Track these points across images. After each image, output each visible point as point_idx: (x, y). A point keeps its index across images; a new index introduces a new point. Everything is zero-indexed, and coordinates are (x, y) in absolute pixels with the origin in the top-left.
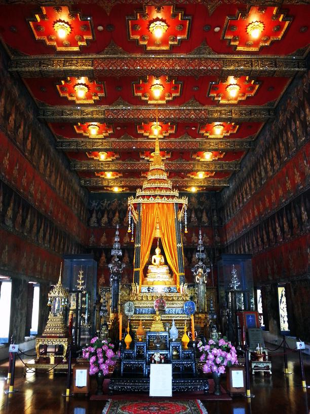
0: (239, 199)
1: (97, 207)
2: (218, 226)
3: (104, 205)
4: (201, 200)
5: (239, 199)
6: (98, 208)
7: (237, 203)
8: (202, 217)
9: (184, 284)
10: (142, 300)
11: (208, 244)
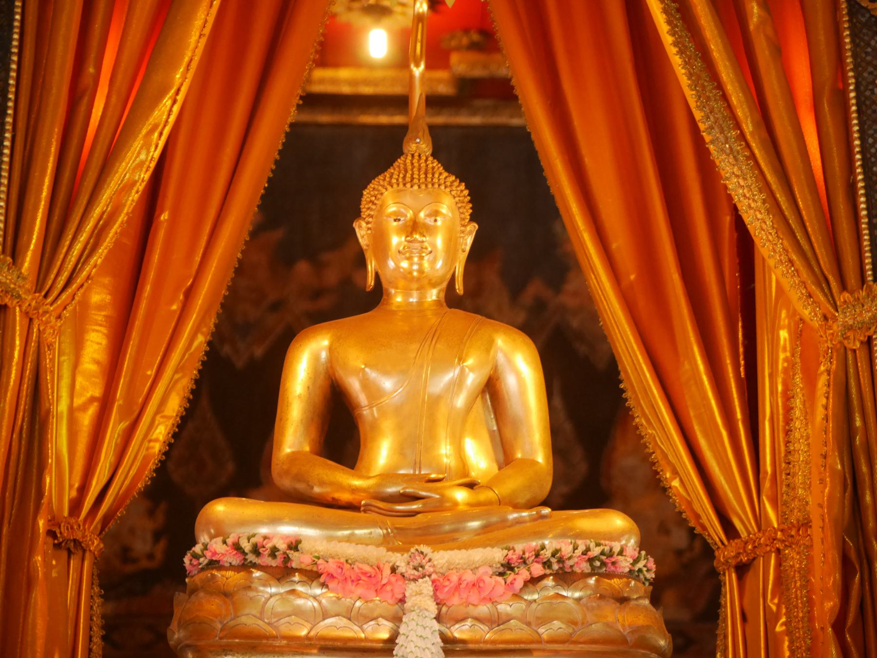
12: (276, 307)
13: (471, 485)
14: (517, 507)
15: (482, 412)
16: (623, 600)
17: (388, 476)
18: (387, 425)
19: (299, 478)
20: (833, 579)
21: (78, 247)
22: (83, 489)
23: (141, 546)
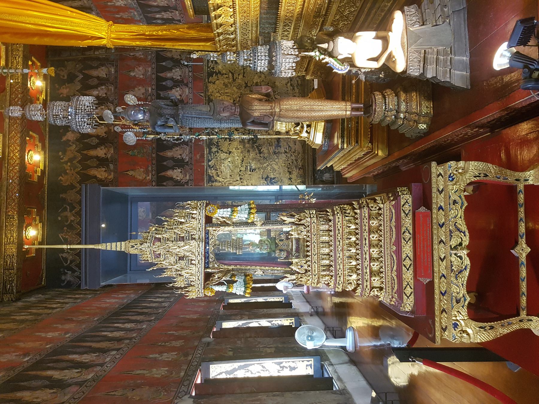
3: (71, 257)
4: (66, 78)
8: (98, 78)
11: (150, 69)
12: (73, 175)
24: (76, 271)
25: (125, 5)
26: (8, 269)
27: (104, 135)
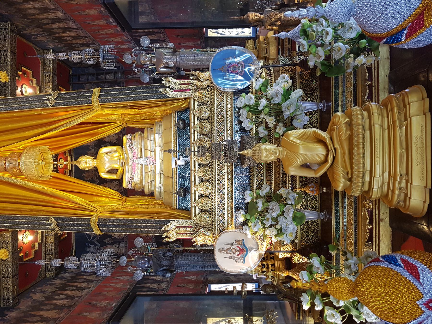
0: (65, 30)
1: (95, 245)
2: (122, 74)
5: (65, 30)
6: (98, 243)
7: (72, 34)
9: (164, 87)
10: (210, 212)
12: (93, 172)
13: (120, 156)
14: (123, 150)
15: (110, 154)
16: (135, 137)
17: (119, 165)
18: (112, 166)
19: (120, 176)
20: (133, 110)
21: (90, 207)
22: (120, 199)
23: (117, 183)
24: (97, 245)
25: (128, 47)
26: (48, 254)
27: (116, 141)
